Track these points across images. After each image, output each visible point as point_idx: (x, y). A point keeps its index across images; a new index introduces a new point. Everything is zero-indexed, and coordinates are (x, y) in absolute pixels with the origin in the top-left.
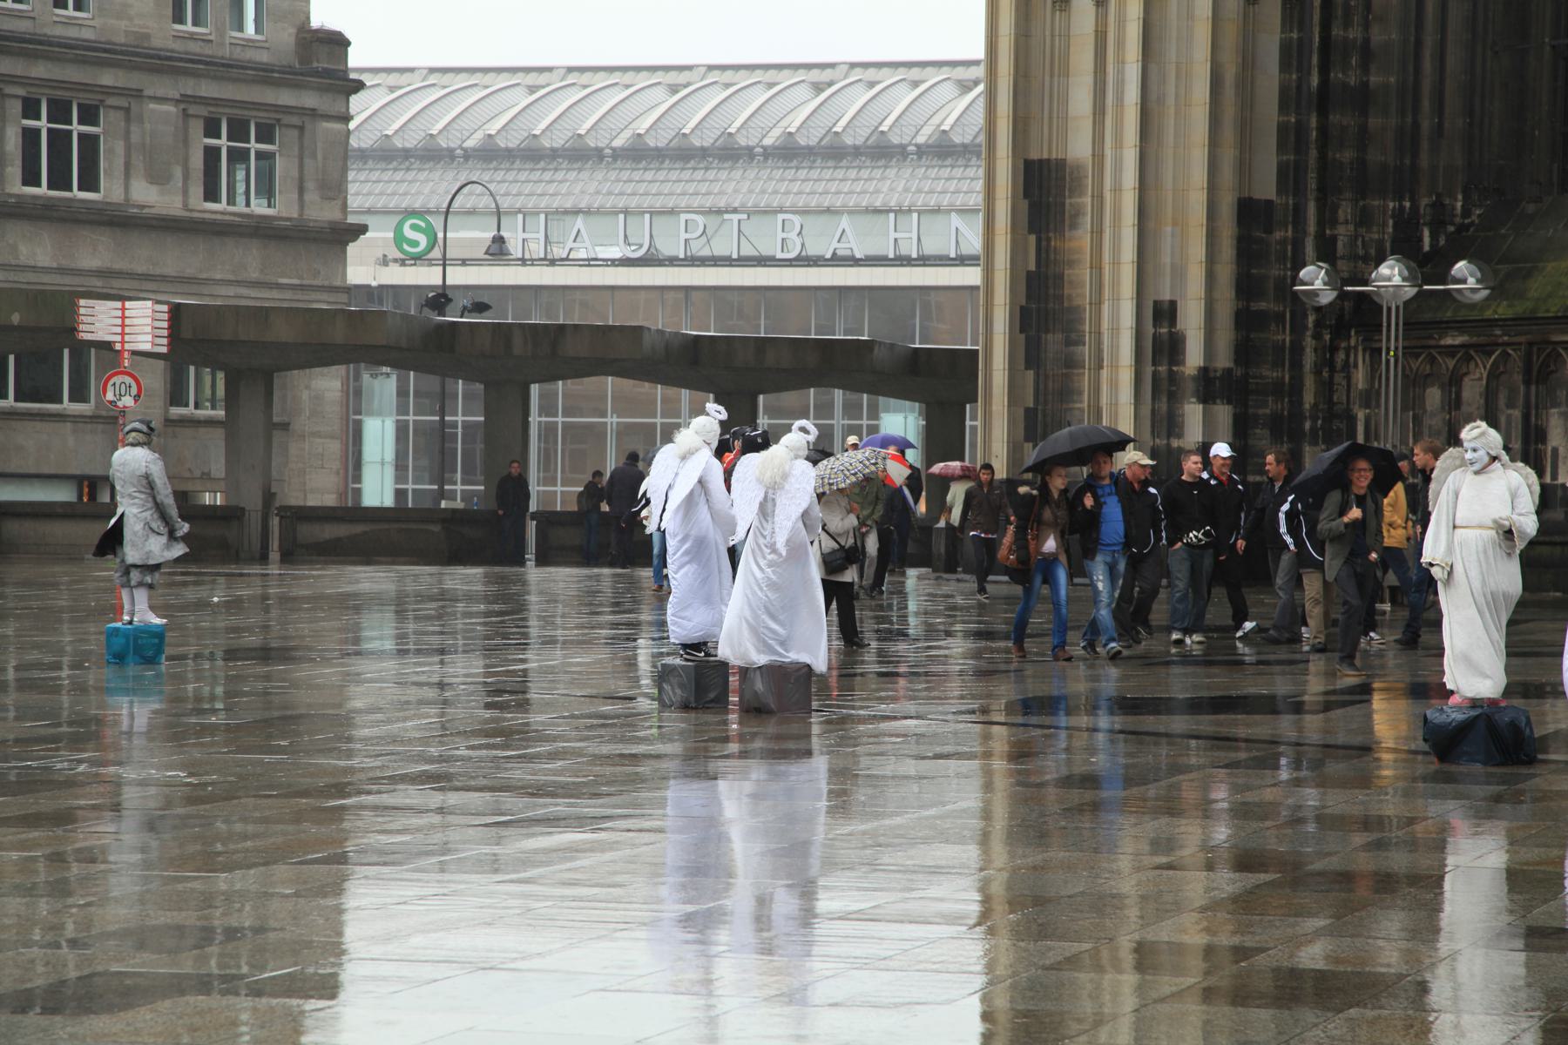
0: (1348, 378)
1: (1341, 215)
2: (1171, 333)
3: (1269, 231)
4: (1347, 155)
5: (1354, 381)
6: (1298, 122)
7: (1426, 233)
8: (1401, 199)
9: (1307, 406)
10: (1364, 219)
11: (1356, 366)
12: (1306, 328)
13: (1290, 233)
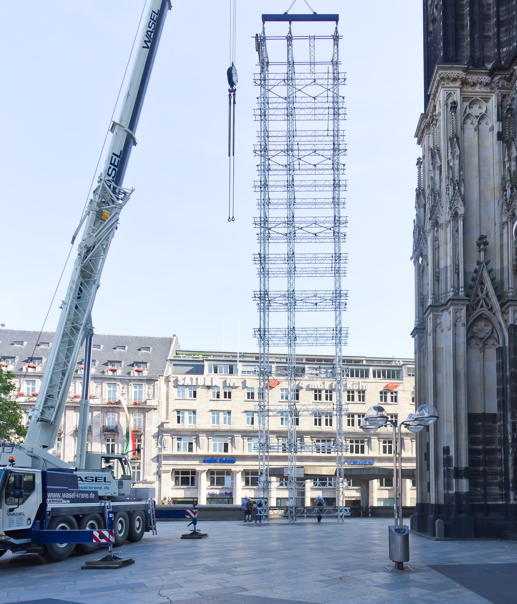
2: (447, 456)
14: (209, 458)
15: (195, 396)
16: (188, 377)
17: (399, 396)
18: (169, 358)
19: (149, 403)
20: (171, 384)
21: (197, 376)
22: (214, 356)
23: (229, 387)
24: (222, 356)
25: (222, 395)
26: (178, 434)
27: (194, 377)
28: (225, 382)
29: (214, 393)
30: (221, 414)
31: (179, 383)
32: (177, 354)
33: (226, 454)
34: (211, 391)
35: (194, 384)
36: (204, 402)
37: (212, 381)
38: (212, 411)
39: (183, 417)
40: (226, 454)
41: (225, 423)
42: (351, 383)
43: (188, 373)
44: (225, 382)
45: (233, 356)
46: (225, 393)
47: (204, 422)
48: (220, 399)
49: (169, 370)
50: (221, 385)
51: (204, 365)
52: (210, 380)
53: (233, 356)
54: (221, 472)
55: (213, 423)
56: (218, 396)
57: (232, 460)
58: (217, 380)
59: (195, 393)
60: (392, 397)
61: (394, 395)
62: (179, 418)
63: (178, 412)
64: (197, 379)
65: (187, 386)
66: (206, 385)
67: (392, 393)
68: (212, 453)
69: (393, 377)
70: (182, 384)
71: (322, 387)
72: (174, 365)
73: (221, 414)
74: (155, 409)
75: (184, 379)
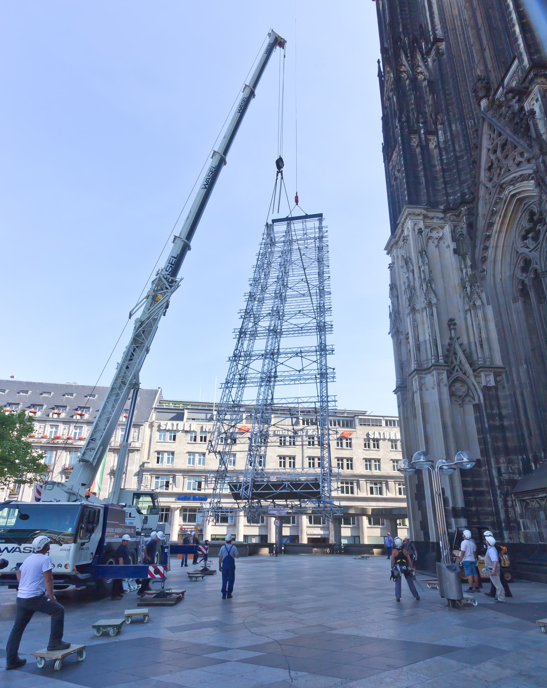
0: (514, 509)
1: (501, 461)
3: (481, 468)
4: (500, 444)
5: (516, 510)
6: (483, 437)
7: (533, 464)
8: (522, 456)
9: (502, 519)
10: (510, 462)
11: (516, 505)
12: (497, 495)
13: (487, 467)
14: (183, 496)
15: (174, 439)
16: (170, 423)
17: (353, 442)
18: (154, 406)
19: (133, 445)
20: (155, 428)
21: (178, 422)
22: (192, 405)
23: (206, 431)
24: (199, 406)
25: (198, 439)
26: (157, 473)
27: (175, 423)
28: (202, 428)
29: (191, 437)
30: (197, 455)
31: (161, 428)
32: (160, 403)
33: (199, 492)
34: (189, 435)
35: (175, 429)
36: (182, 445)
37: (190, 427)
38: (188, 452)
39: (162, 458)
40: (199, 492)
41: (200, 463)
42: (312, 430)
43: (173, 419)
44: (202, 428)
45: (208, 406)
46: (201, 437)
47: (181, 463)
48: (197, 442)
49: (153, 416)
50: (198, 431)
51: (184, 413)
52: (189, 425)
53: (208, 406)
54: (193, 510)
55: (189, 463)
56: (195, 440)
57: (204, 498)
58: (195, 426)
59: (175, 436)
60: (347, 443)
61: (349, 441)
62: (158, 458)
63: (158, 453)
64: (177, 424)
65: (168, 431)
66: (185, 430)
67: (347, 440)
68: (186, 491)
69: (347, 426)
70: (164, 428)
71: (286, 434)
72: (158, 412)
73: (197, 455)
74: (138, 450)
75: (166, 425)
